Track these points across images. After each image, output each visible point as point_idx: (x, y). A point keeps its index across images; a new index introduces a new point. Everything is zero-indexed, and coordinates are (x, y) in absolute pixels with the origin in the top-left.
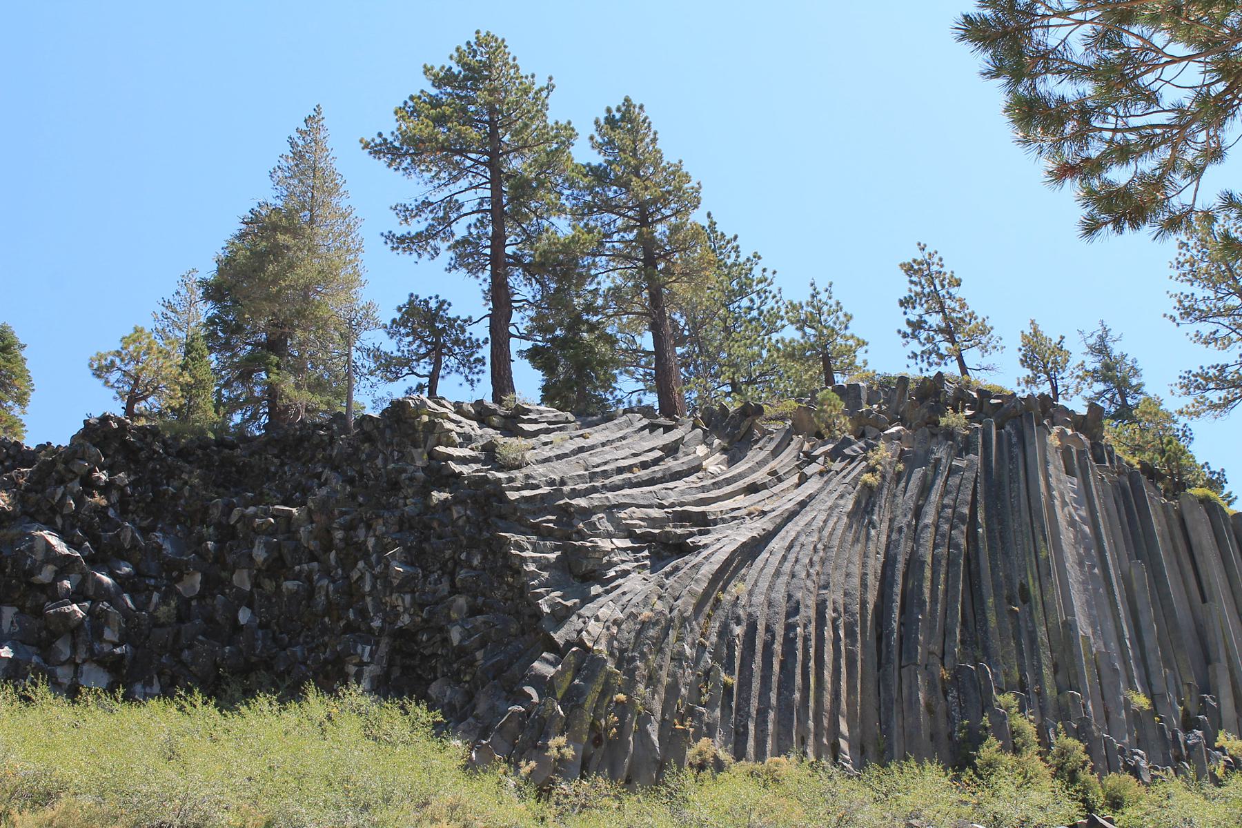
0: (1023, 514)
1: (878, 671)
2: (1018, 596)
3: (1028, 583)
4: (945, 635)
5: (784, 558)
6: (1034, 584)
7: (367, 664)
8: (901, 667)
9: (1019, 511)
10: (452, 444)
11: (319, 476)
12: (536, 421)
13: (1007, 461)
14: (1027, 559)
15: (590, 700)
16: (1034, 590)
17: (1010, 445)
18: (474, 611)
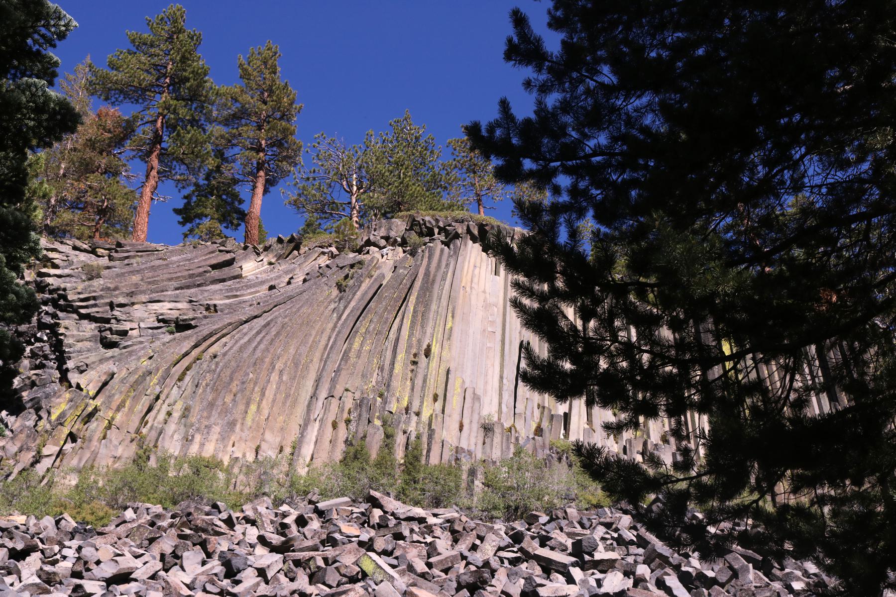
0: (442, 300)
5: (258, 333)
12: (128, 251)
15: (69, 420)
16: (435, 349)
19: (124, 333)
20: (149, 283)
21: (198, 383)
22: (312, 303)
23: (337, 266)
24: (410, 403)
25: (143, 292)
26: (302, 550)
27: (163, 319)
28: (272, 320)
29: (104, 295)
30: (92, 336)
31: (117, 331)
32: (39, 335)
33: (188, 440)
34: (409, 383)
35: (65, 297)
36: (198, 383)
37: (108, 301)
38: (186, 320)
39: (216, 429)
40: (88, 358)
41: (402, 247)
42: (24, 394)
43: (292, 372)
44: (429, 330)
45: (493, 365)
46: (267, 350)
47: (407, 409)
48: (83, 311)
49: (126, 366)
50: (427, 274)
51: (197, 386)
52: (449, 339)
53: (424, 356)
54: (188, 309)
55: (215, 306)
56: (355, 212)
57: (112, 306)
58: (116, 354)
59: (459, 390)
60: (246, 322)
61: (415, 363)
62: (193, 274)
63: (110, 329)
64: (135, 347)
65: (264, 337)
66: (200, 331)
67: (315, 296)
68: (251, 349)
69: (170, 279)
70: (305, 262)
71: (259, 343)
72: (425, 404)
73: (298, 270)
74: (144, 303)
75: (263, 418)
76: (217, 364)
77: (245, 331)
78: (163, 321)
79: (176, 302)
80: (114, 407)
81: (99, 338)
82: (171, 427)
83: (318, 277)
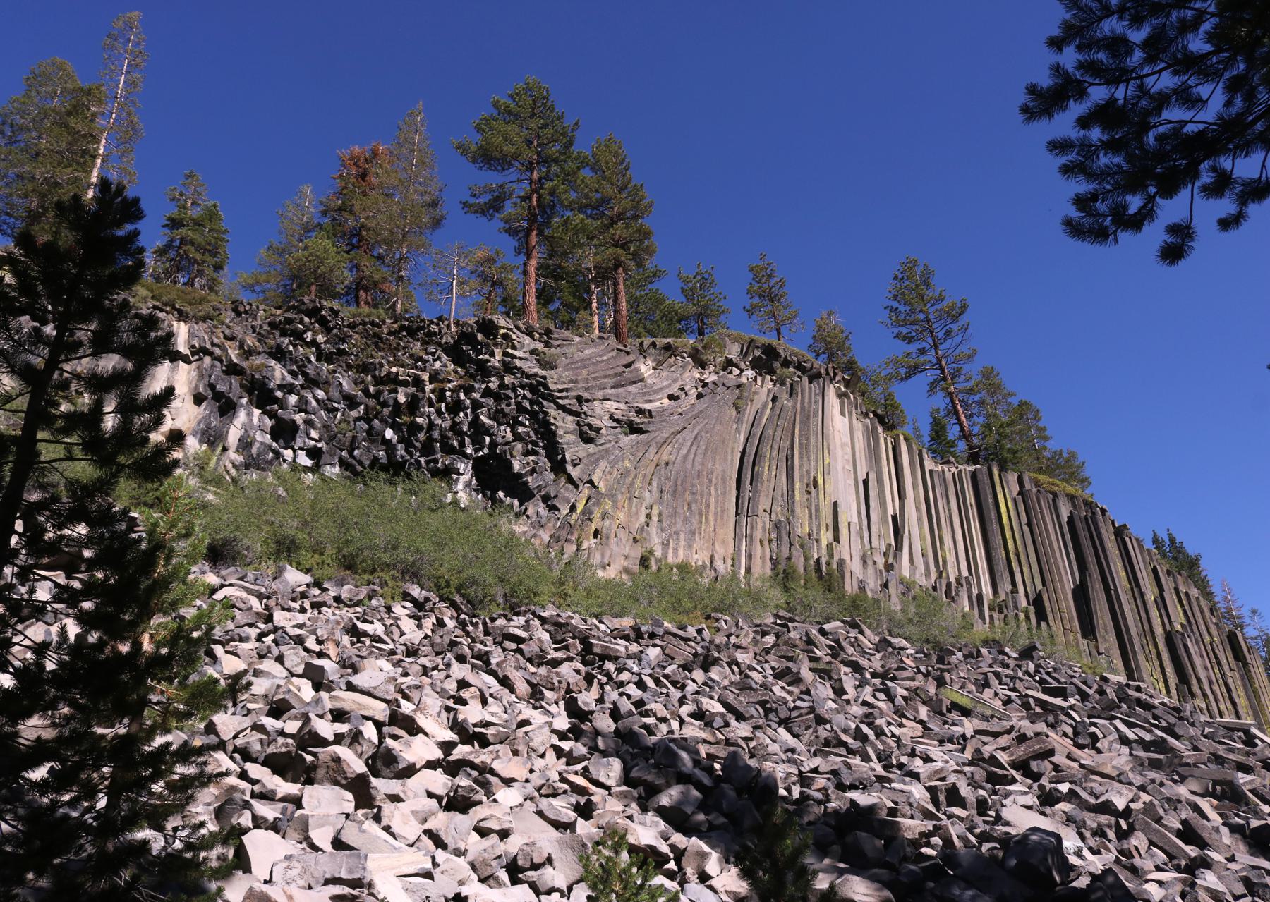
5: (692, 445)
10: (514, 347)
11: (433, 354)
12: (557, 339)
16: (820, 482)
17: (815, 394)
18: (527, 453)
19: (598, 430)
20: (595, 379)
23: (724, 385)
24: (811, 529)
25: (593, 387)
26: (903, 679)
30: (575, 430)
32: (520, 419)
33: (665, 545)
35: (546, 387)
38: (638, 424)
39: (682, 536)
42: (530, 479)
44: (813, 463)
47: (809, 535)
48: (561, 402)
50: (803, 408)
52: (829, 473)
57: (580, 399)
61: (809, 493)
63: (590, 426)
64: (607, 446)
69: (605, 377)
71: (695, 454)
75: (712, 529)
77: (680, 441)
78: (617, 421)
82: (653, 530)
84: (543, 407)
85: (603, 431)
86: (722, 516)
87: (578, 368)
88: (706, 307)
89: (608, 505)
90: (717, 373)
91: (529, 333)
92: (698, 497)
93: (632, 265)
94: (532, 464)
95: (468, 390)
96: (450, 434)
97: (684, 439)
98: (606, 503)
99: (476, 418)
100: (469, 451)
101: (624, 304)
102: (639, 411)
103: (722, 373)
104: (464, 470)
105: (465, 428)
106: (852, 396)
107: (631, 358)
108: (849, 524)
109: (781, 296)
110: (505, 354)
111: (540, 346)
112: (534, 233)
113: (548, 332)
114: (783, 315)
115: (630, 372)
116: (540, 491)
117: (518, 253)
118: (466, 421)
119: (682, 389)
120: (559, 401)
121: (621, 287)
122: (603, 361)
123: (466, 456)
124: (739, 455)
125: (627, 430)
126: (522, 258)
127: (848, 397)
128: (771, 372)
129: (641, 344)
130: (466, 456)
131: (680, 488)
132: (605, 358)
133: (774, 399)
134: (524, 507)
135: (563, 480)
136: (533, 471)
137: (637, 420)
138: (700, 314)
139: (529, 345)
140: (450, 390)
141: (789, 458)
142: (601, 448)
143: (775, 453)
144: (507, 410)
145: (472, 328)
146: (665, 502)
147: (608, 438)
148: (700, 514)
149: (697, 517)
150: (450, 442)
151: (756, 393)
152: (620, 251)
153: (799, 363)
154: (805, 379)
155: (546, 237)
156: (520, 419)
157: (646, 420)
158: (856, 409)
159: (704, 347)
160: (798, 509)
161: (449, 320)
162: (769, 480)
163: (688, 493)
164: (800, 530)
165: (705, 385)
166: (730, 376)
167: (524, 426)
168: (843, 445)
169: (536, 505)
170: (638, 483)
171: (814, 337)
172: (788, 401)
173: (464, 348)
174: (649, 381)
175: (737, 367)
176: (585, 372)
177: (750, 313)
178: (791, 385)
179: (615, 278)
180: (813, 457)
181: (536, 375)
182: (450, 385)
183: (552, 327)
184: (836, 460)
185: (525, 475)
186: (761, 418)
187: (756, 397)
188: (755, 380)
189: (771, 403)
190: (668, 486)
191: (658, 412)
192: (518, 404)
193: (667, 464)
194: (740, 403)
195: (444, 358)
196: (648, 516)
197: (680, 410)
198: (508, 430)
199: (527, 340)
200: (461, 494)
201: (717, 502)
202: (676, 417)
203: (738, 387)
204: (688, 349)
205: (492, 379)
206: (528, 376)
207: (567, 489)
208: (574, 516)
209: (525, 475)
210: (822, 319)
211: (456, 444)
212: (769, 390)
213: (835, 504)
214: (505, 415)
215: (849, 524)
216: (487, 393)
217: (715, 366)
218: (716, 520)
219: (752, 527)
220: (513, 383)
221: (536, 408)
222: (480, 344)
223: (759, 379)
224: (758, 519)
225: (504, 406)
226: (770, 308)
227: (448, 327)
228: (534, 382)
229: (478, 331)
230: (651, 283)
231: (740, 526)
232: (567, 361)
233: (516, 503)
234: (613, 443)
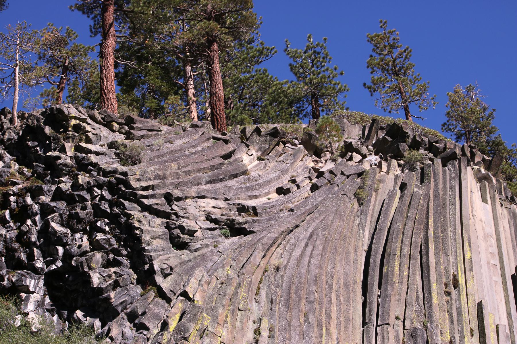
0: (457, 227)
1: (363, 327)
2: (451, 283)
3: (458, 273)
4: (406, 306)
5: (306, 245)
6: (462, 276)
7: (33, 293)
8: (377, 325)
9: (455, 225)
12: (141, 129)
13: (448, 190)
14: (458, 258)
15: (192, 334)
17: (451, 178)
18: (107, 264)
19: (192, 233)
20: (187, 173)
21: (272, 298)
22: (340, 216)
23: (342, 173)
24: (452, 337)
25: (185, 183)
27: (216, 219)
28: (313, 232)
29: (160, 184)
30: (164, 234)
31: (189, 230)
32: (99, 224)
34: (447, 315)
35: (127, 184)
36: (272, 298)
37: (162, 191)
40: (168, 259)
41: (397, 160)
42: (112, 294)
43: (345, 293)
44: (452, 259)
45: (501, 300)
46: (320, 267)
48: (146, 201)
49: (215, 274)
50: (436, 195)
51: (272, 302)
52: (471, 270)
53: (453, 287)
54: (226, 209)
55: (254, 208)
56: (192, 83)
57: (169, 198)
58: (191, 257)
59: (494, 327)
60: (291, 231)
61: (448, 294)
62: (213, 166)
63: (182, 228)
64: (204, 251)
65: (312, 251)
66: (261, 239)
67: (340, 208)
68: (306, 264)
69: (199, 170)
70: (295, 161)
71: (311, 256)
72: (466, 338)
73: (290, 170)
74: (194, 198)
76: (282, 278)
78: (216, 221)
79: (215, 199)
80: (222, 324)
81: (168, 236)
83: (327, 184)
84: (125, 208)
85: (199, 234)
86: (346, 328)
87: (166, 162)
88: (319, 86)
89: (207, 321)
90: (334, 160)
91: (107, 124)
92: (317, 306)
93: (228, 39)
94: (114, 277)
95: (36, 193)
96: (16, 245)
97: (297, 239)
98: (203, 318)
99: (46, 225)
100: (39, 264)
101: (221, 86)
102: (242, 209)
103: (340, 160)
104: (35, 286)
105: (34, 238)
106: (494, 179)
107: (230, 148)
108: (497, 327)
109: (408, 69)
110: (78, 149)
111: (120, 138)
112: (111, 9)
113: (130, 121)
114: (411, 89)
115: (229, 164)
116: (125, 308)
117: (94, 32)
118: (34, 230)
119: (293, 181)
120: (143, 200)
121: (217, 66)
122: (197, 152)
123: (36, 271)
124: (364, 254)
125: (227, 231)
126: (99, 38)
127: (490, 180)
128: (398, 156)
129: (243, 131)
130: (36, 271)
131: (294, 296)
132: (199, 149)
133: (403, 187)
134: (106, 328)
135: (152, 294)
136: (116, 285)
137: (240, 219)
138: (314, 95)
139: (107, 137)
140: (14, 194)
141: (424, 255)
142: (197, 254)
143: (406, 250)
144: (82, 214)
145: (38, 121)
146: (277, 315)
147: (205, 241)
148: (320, 326)
149: (316, 330)
150: (17, 255)
151: (381, 181)
152: (213, 24)
153: (431, 143)
154: (438, 161)
155: (126, 13)
156: (99, 224)
157: (250, 219)
158: (500, 193)
159: (318, 131)
160: (436, 314)
161: (12, 113)
162: (401, 282)
163: (303, 301)
164: (439, 338)
165: (320, 174)
166: (350, 163)
167: (104, 232)
168: (486, 236)
169: (121, 325)
170: (243, 292)
171: (448, 113)
172: (417, 186)
173: (30, 144)
174: (253, 174)
175: (358, 152)
176: (174, 166)
177: (372, 89)
178: (422, 169)
179: (209, 56)
180: (451, 252)
181: (115, 171)
182: (15, 189)
183: (135, 115)
184: (479, 254)
185: (106, 289)
186: (388, 210)
187: (381, 186)
188: (380, 166)
189: (399, 192)
190: (280, 295)
191: (264, 209)
192: (95, 207)
193: (277, 269)
194: (363, 194)
195: (8, 157)
196: (257, 332)
197: (291, 206)
198: (85, 238)
199: (104, 132)
200: (32, 315)
201: (339, 311)
202: (287, 213)
203: (360, 175)
204: (300, 135)
205: (64, 179)
206: (106, 174)
207: (157, 304)
208: (166, 335)
209: (106, 289)
210: (456, 92)
211: (23, 257)
212: (397, 177)
213: (480, 306)
214: (80, 220)
215: (497, 327)
216: (58, 195)
217: (332, 153)
218: (339, 332)
219: (383, 338)
220: (88, 183)
221: (116, 210)
222: (48, 138)
223: (384, 165)
224: (390, 329)
225: (78, 210)
226: (395, 83)
227: (12, 121)
228: (113, 179)
229: (45, 124)
230: (258, 63)
231: (369, 338)
232: (153, 154)
233: (97, 323)
234: (211, 248)
